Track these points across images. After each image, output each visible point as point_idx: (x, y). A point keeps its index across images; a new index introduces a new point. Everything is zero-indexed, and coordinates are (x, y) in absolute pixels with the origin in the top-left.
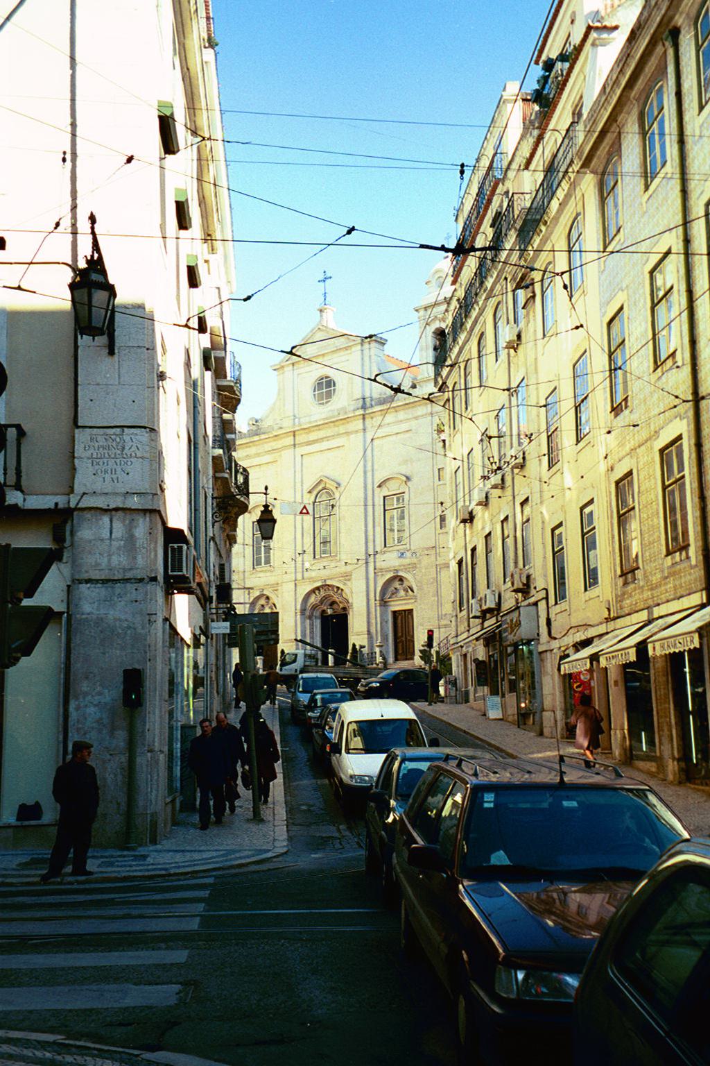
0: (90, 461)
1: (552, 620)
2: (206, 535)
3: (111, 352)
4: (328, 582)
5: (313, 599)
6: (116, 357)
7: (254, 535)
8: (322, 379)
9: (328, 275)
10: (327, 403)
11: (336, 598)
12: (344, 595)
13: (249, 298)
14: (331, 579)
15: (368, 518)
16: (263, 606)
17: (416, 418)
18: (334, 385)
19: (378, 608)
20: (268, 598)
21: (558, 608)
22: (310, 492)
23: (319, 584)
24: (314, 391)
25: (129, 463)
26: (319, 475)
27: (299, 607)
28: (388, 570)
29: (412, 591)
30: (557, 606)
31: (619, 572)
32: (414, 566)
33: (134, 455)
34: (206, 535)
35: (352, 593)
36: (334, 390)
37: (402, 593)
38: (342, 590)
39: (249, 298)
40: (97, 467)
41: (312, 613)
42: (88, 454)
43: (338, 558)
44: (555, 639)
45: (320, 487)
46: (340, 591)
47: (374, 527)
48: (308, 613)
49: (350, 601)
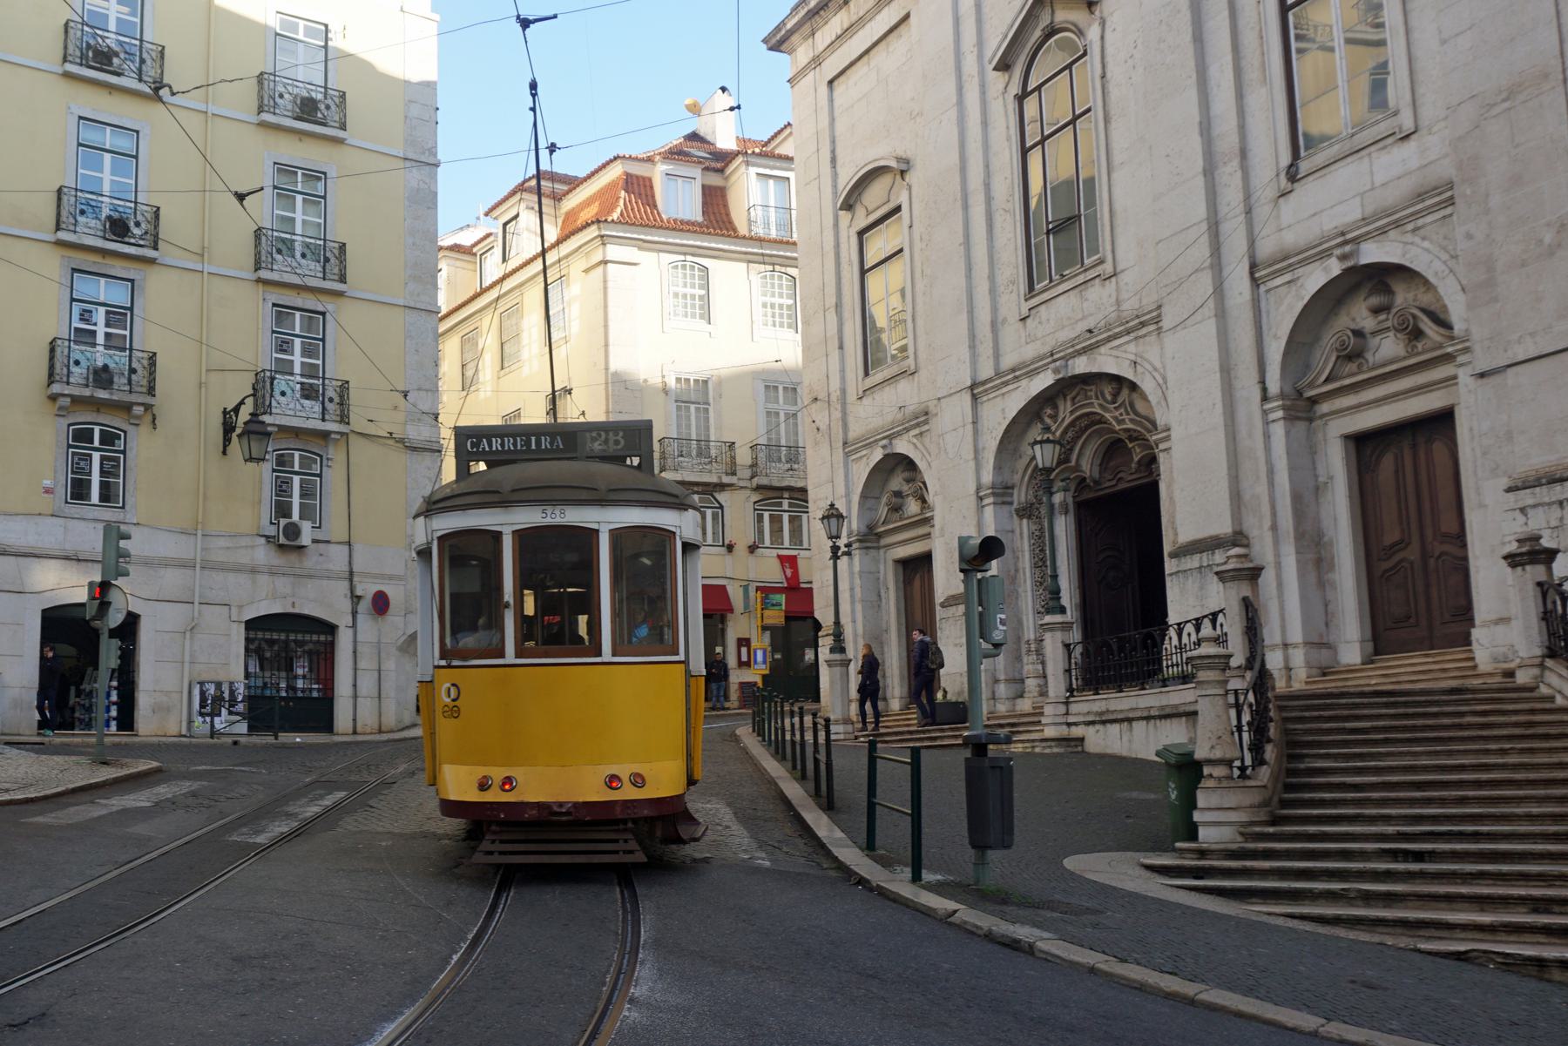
4: (1081, 366)
11: (1117, 419)
12: (1140, 406)
14: (1080, 353)
15: (1213, 71)
16: (898, 494)
19: (1278, 430)
20: (908, 464)
22: (1004, 65)
23: (1045, 380)
27: (987, 477)
28: (1316, 253)
29: (1443, 323)
35: (1163, 386)
37: (1388, 347)
38: (1133, 386)
43: (1108, 268)
46: (1125, 392)
47: (1240, 95)
48: (1020, 496)
49: (1161, 421)
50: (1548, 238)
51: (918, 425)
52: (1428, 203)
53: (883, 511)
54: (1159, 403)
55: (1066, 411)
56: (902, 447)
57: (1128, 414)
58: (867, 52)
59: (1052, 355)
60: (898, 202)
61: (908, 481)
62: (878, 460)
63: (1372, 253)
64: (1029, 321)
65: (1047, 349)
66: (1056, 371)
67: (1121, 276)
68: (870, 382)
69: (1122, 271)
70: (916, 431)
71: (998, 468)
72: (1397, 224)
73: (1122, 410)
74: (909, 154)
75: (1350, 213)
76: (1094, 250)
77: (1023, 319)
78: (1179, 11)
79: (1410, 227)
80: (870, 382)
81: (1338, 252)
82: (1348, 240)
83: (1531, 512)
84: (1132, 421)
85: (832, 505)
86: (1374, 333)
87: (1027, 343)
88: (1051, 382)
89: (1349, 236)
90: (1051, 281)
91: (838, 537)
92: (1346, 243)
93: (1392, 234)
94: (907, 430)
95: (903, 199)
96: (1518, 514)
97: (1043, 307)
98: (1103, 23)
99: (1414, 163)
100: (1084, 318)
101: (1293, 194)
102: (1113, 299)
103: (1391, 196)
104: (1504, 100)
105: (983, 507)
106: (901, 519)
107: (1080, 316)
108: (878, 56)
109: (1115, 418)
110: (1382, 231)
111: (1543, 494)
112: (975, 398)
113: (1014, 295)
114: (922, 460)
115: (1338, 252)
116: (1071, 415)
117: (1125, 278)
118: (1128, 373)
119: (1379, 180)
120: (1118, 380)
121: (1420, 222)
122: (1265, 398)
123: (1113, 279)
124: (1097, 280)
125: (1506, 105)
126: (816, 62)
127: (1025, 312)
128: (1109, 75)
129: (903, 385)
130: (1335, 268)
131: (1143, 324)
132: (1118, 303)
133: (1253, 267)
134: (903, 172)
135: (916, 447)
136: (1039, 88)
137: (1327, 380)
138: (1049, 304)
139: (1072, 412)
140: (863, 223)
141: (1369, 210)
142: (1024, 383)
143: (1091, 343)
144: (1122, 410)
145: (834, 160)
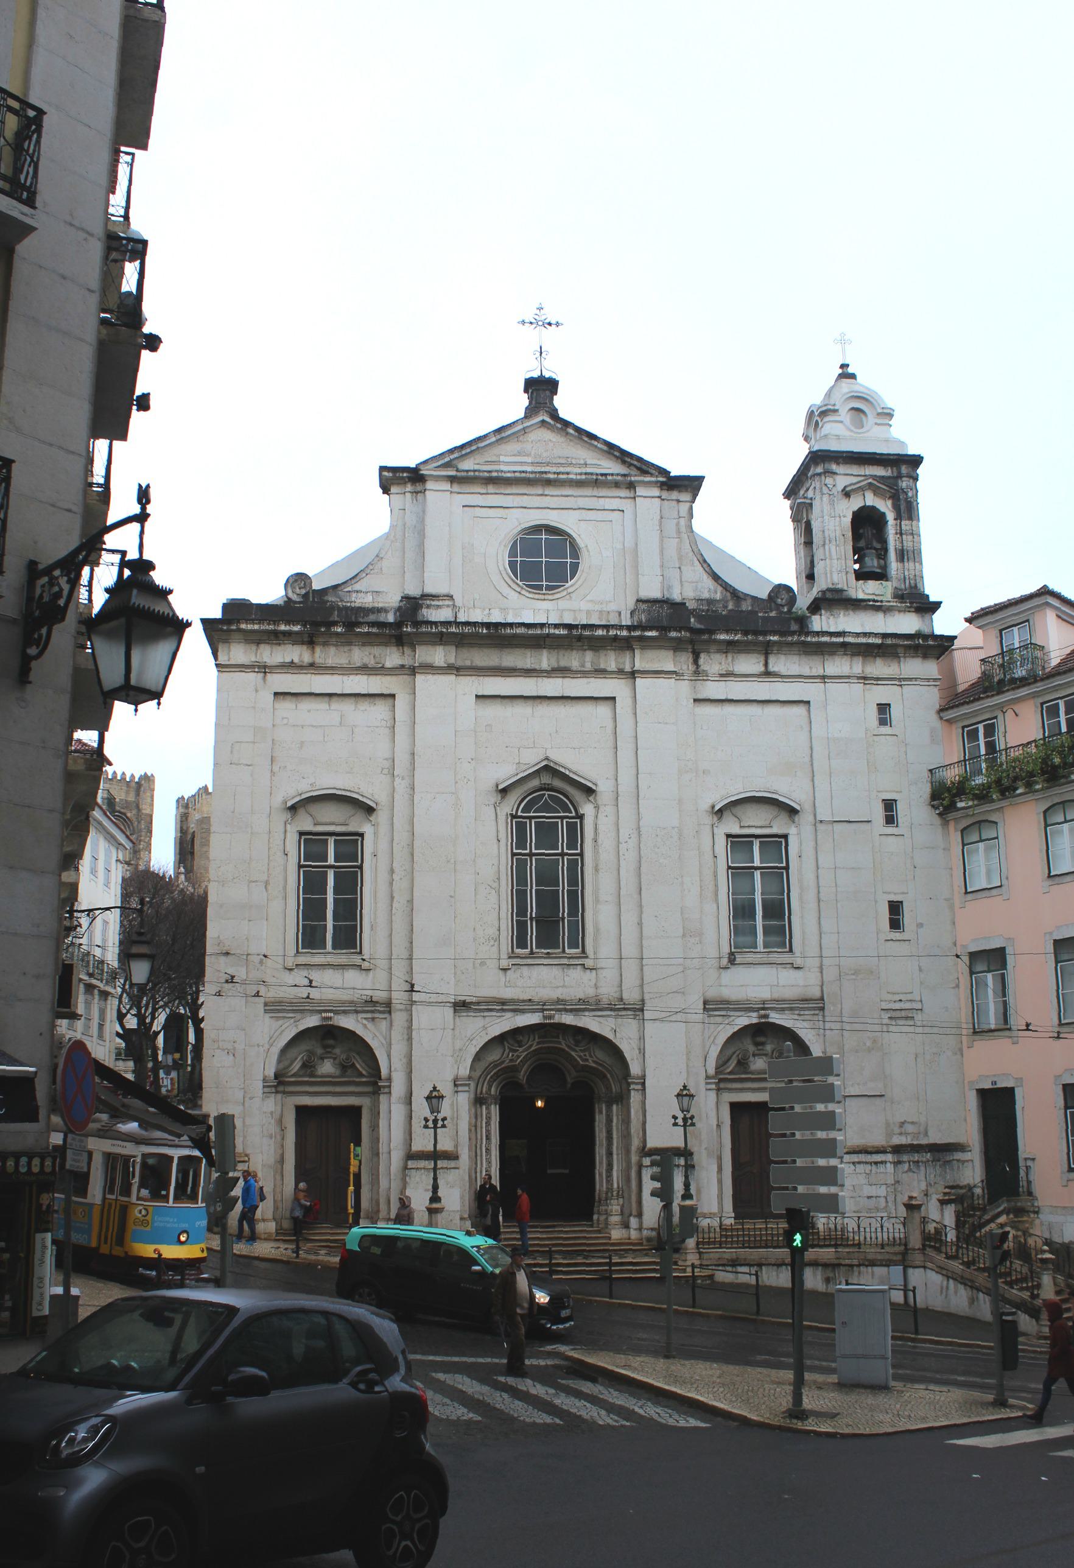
4: (568, 1019)
5: (495, 1056)
7: (300, 866)
10: (549, 588)
17: (824, 678)
22: (504, 792)
28: (744, 1007)
32: (815, 1005)
45: (535, 783)
50: (868, 1044)
51: (372, 1012)
52: (810, 1005)
53: (296, 1066)
54: (633, 1059)
56: (347, 1022)
57: (591, 1056)
58: (330, 695)
59: (543, 1005)
60: (361, 830)
61: (325, 1047)
62: (311, 1025)
63: (775, 1018)
64: (509, 972)
66: (545, 1017)
67: (600, 971)
68: (302, 960)
69: (602, 968)
70: (369, 1015)
72: (791, 1009)
73: (587, 1053)
75: (765, 994)
77: (505, 970)
78: (671, 837)
79: (797, 1012)
80: (302, 960)
81: (762, 1012)
82: (763, 1006)
83: (857, 1165)
84: (594, 1062)
85: (435, 1088)
86: (754, 1055)
87: (506, 987)
88: (538, 1021)
89: (766, 1006)
90: (532, 953)
91: (438, 1112)
92: (763, 1009)
93: (786, 1012)
94: (357, 1012)
95: (367, 829)
96: (851, 1165)
97: (525, 969)
98: (597, 807)
99: (801, 983)
100: (564, 986)
101: (729, 970)
102: (594, 981)
103: (788, 994)
104: (853, 974)
105: (457, 1092)
106: (312, 1075)
107: (561, 984)
108: (347, 706)
109: (580, 1057)
110: (783, 1009)
111: (862, 1157)
113: (495, 949)
114: (373, 1039)
115: (762, 1012)
116: (538, 1043)
117: (603, 973)
118: (610, 1036)
119: (781, 983)
121: (802, 1013)
122: (707, 1077)
123: (594, 971)
124: (579, 967)
125: (854, 977)
126: (264, 669)
127: (504, 963)
128: (600, 841)
129: (352, 978)
130: (753, 1019)
131: (625, 1009)
132: (596, 987)
133: (705, 1003)
135: (365, 1026)
136: (530, 818)
137: (730, 1073)
138: (532, 967)
139: (538, 1043)
141: (776, 996)
142: (509, 1015)
143: (582, 1006)
144: (587, 1053)
145: (272, 760)
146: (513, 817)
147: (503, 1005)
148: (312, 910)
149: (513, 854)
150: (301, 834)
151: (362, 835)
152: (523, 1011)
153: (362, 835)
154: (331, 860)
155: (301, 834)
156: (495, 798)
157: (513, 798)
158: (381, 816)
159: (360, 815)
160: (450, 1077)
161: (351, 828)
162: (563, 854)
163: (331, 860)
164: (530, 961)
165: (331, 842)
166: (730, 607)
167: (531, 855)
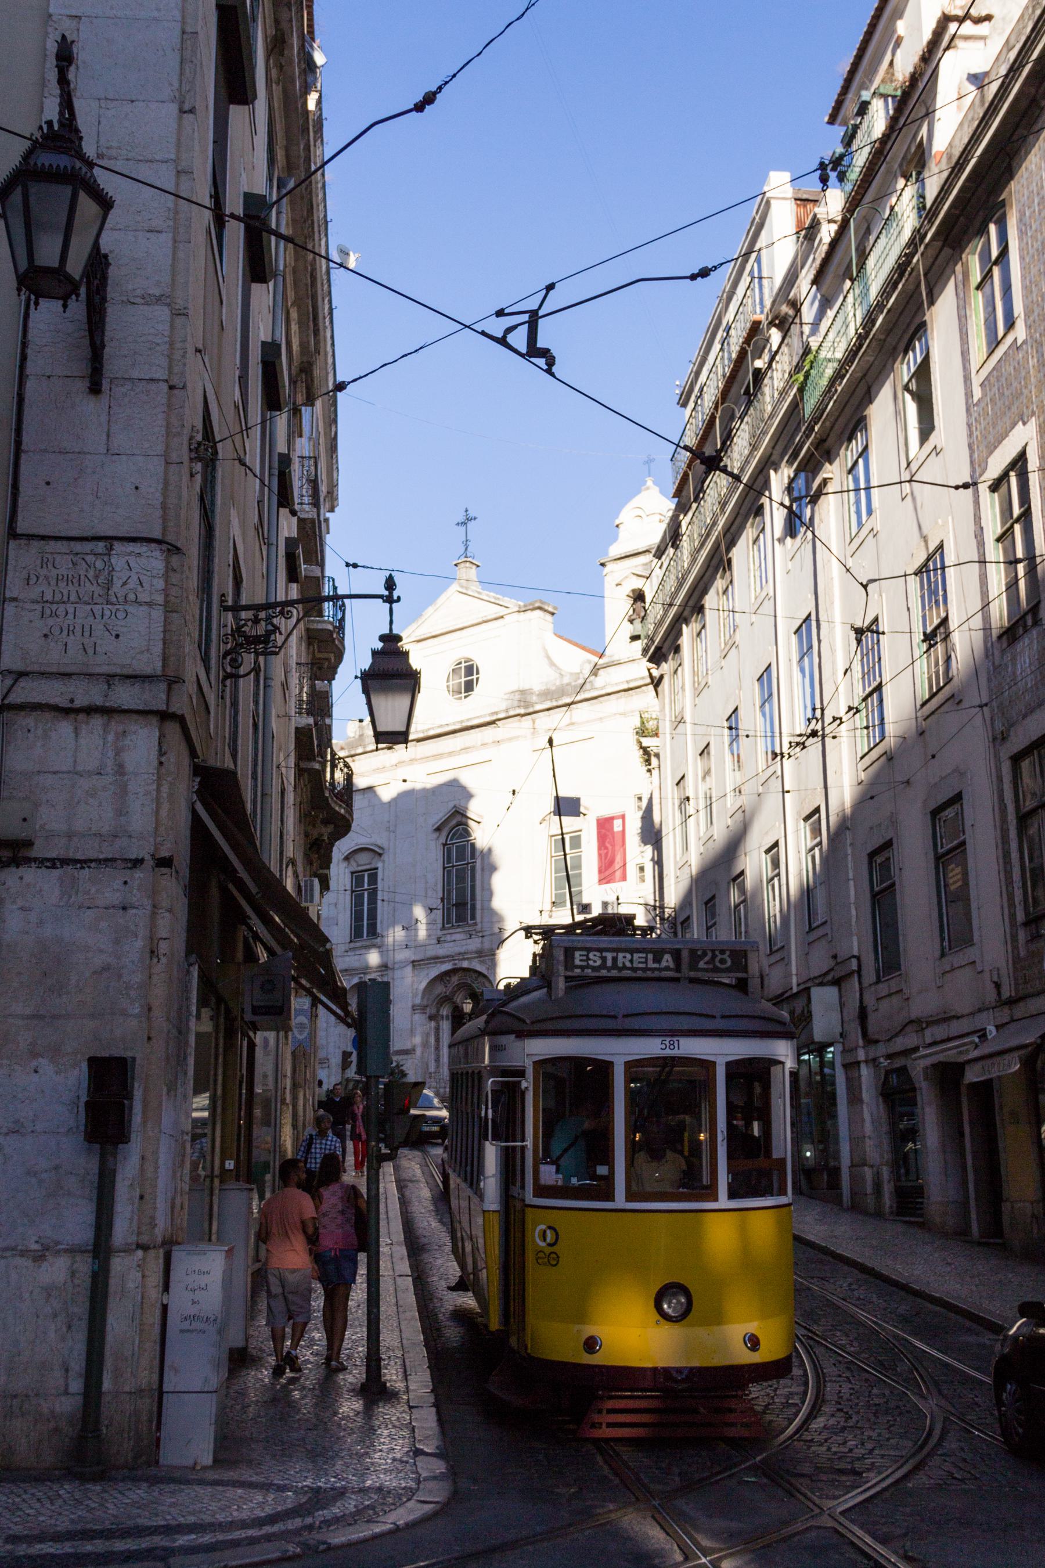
0: (38, 607)
1: (870, 1008)
2: (281, 853)
3: (95, 389)
4: (465, 964)
5: (440, 989)
6: (104, 398)
8: (460, 663)
9: (471, 514)
13: (429, 99)
18: (478, 673)
21: (883, 989)
22: (438, 829)
23: (447, 967)
24: (448, 681)
25: (121, 615)
26: (451, 805)
30: (881, 986)
31: (1020, 916)
33: (132, 597)
34: (281, 853)
36: (477, 679)
38: (485, 976)
39: (429, 99)
40: (51, 622)
41: (438, 1011)
42: (35, 593)
43: (478, 927)
44: (877, 1042)
45: (454, 822)
55: (455, 979)
65: (449, 953)
68: (352, 945)
71: (423, 998)
74: (385, 846)
76: (473, 917)
95: (380, 865)
112: (414, 966)
120: (480, 974)
134: (380, 855)
140: (353, 870)
146: (444, 845)
147: (436, 959)
148: (357, 917)
149: (444, 868)
150: (352, 873)
151: (377, 869)
152: (444, 962)
153: (377, 869)
154: (366, 887)
155: (352, 873)
156: (437, 834)
157: (444, 833)
158: (385, 857)
159: (377, 857)
160: (410, 1005)
161: (373, 866)
162: (467, 864)
163: (366, 887)
164: (451, 931)
165: (366, 874)
166: (558, 683)
167: (453, 866)
